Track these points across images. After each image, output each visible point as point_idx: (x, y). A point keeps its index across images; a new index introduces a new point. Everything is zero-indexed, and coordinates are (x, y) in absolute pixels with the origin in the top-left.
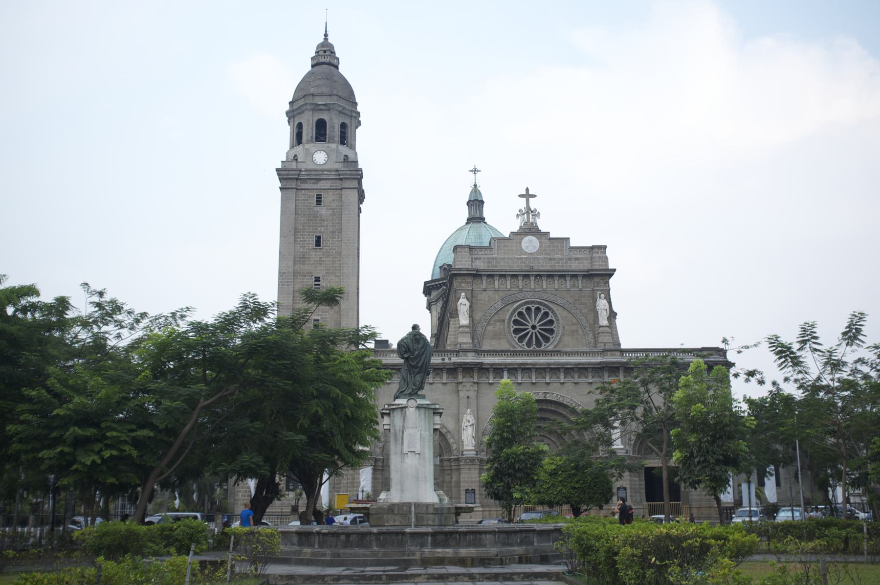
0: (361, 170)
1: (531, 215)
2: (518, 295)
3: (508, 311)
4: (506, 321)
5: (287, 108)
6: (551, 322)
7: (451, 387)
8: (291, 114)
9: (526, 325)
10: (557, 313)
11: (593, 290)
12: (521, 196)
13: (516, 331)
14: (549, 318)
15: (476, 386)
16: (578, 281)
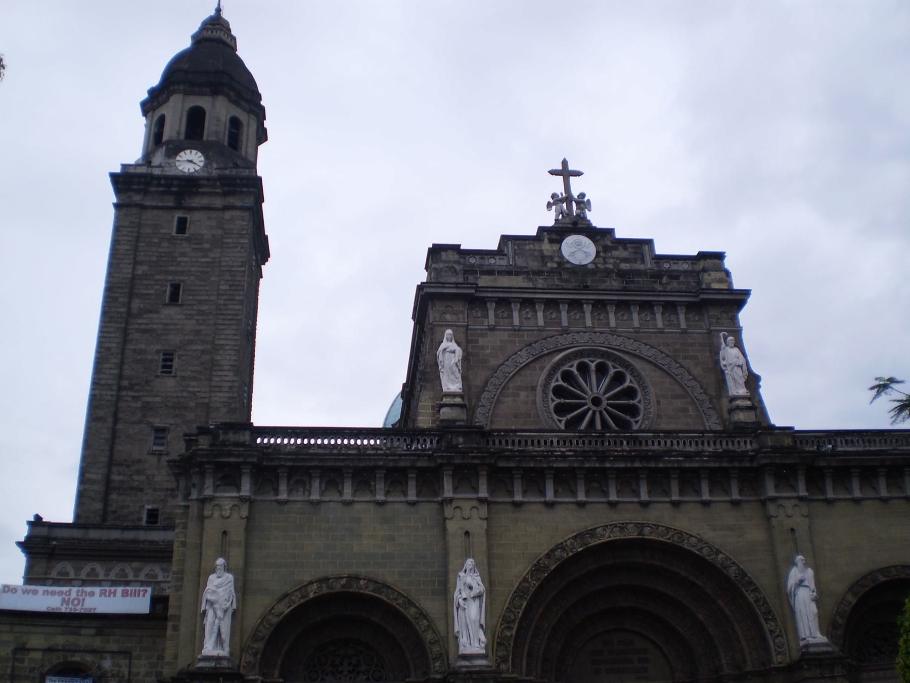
0: (260, 179)
1: (574, 204)
2: (561, 339)
3: (542, 369)
4: (539, 389)
5: (145, 96)
6: (630, 393)
7: (427, 511)
8: (149, 105)
9: (580, 398)
10: (643, 373)
11: (710, 332)
12: (553, 173)
13: (560, 410)
14: (627, 384)
15: (484, 510)
16: (678, 315)
